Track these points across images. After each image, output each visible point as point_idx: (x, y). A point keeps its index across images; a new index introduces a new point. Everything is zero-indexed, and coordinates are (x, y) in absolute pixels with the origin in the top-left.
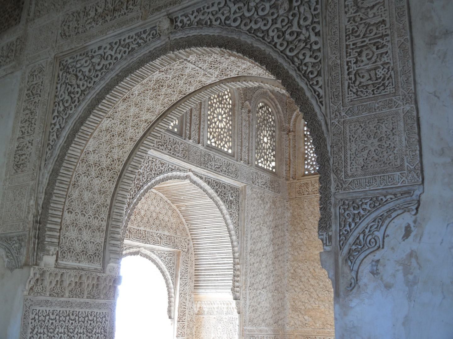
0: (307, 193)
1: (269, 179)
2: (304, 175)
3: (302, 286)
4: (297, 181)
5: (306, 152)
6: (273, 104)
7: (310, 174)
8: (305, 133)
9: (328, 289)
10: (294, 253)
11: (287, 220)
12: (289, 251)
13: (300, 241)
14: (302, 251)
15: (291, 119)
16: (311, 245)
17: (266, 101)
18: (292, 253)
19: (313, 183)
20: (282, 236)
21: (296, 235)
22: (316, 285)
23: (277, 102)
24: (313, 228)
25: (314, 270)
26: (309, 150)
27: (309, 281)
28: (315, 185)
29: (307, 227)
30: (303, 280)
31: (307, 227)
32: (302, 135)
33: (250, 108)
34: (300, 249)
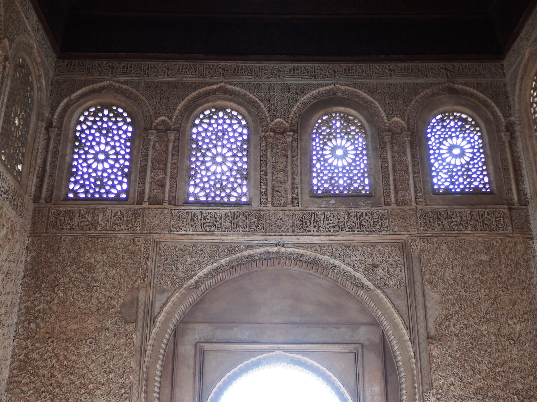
0: (69, 227)
1: (13, 187)
2: (67, 199)
3: (38, 384)
4: (53, 206)
5: (75, 163)
6: (37, 71)
7: (77, 198)
8: (78, 134)
9: (88, 390)
10: (29, 324)
11: (23, 269)
12: (21, 320)
13: (43, 304)
14: (46, 322)
15: (57, 107)
16: (65, 313)
17: (28, 61)
18: (26, 324)
19: (82, 212)
20: (13, 293)
21: (38, 295)
22: (65, 381)
23: (42, 73)
24: (71, 285)
25: (65, 356)
26: (80, 161)
27: (54, 376)
28: (86, 216)
29: (61, 282)
30: (41, 372)
31: (61, 282)
32: (71, 135)
33: (9, 54)
34: (43, 319)
